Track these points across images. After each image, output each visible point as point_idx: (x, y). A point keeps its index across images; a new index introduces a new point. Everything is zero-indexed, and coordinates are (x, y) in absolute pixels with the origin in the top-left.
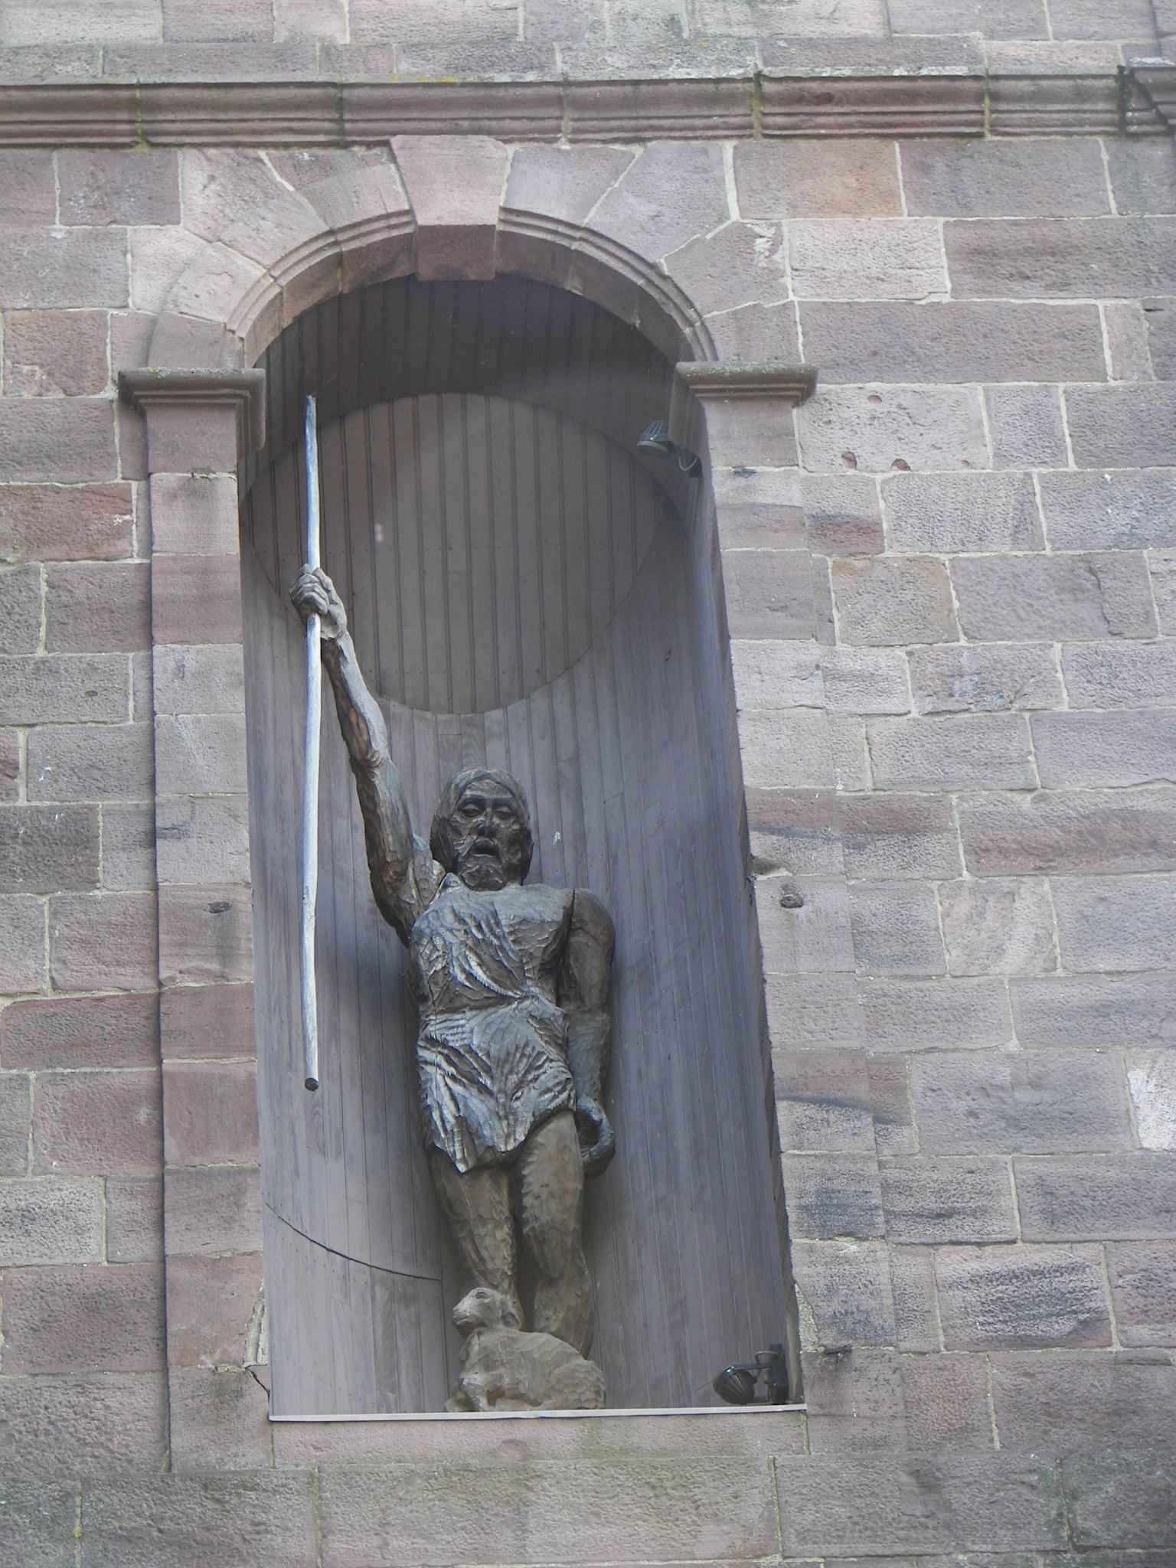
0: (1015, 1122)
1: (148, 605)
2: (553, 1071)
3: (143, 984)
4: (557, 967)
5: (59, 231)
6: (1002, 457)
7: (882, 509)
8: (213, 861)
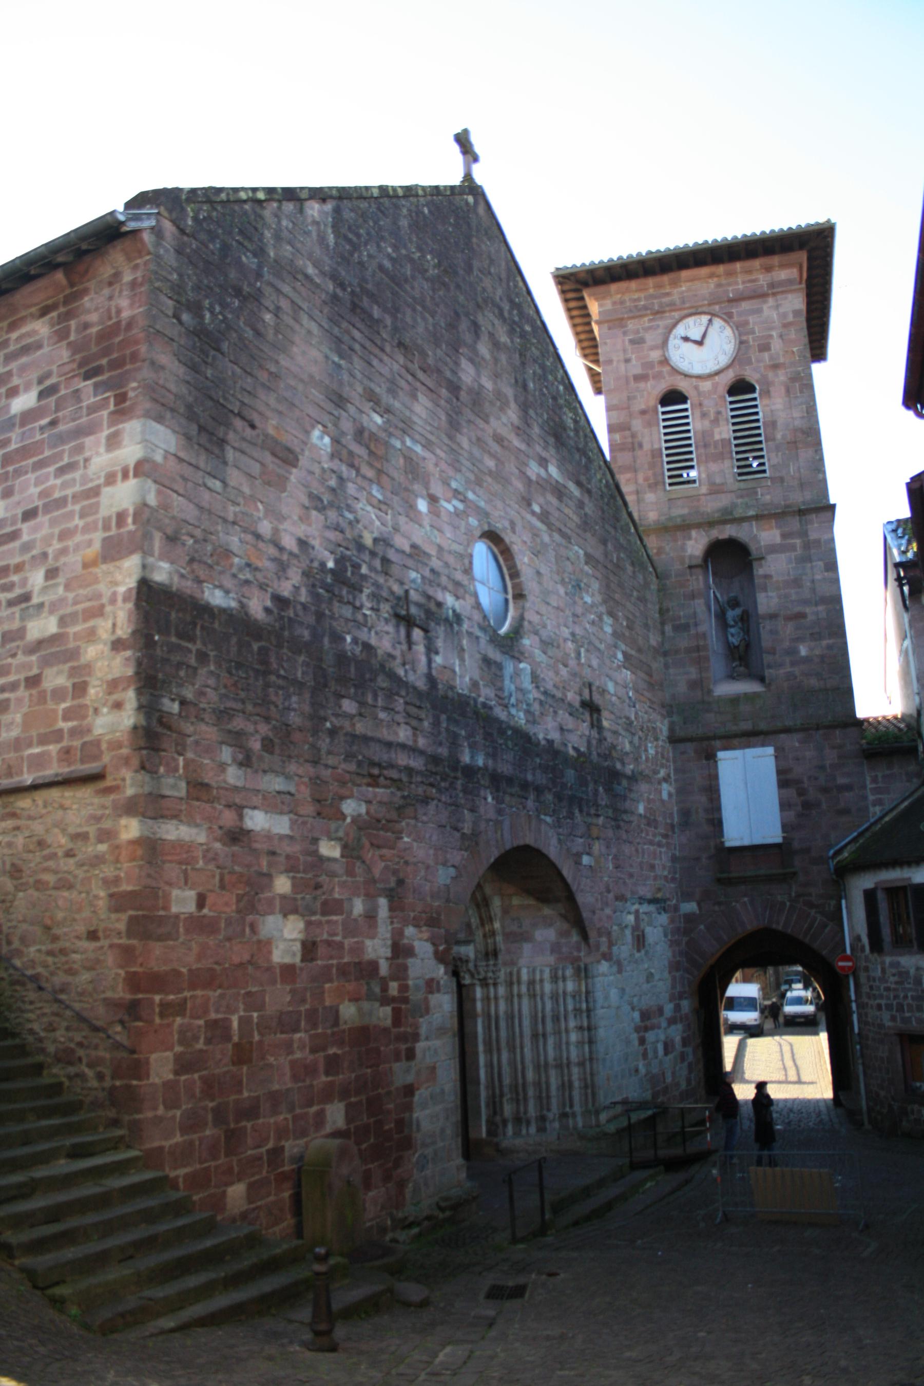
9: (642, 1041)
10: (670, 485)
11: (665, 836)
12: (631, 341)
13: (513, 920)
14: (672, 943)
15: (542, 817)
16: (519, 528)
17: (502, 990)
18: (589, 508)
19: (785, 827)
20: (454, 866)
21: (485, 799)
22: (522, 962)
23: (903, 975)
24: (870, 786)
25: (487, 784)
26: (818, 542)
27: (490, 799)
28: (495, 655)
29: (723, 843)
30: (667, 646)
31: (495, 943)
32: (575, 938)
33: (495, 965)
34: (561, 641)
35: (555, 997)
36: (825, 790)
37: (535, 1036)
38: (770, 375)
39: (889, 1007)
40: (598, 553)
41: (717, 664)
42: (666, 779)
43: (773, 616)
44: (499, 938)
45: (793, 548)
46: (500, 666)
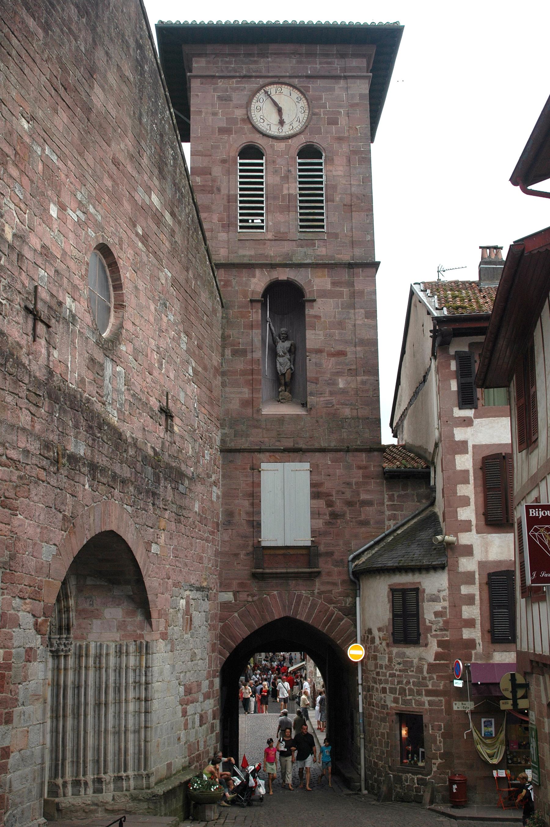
0: (328, 384)
1: (252, 325)
2: (289, 364)
3: (251, 368)
4: (290, 351)
5: (244, 279)
6: (334, 309)
7: (322, 315)
8: (258, 355)
9: (184, 713)
10: (241, 227)
11: (212, 533)
12: (219, 97)
13: (86, 598)
14: (212, 627)
15: (125, 506)
16: (125, 246)
17: (71, 662)
18: (178, 238)
19: (314, 533)
20: (55, 545)
21: (84, 486)
22: (92, 637)
23: (407, 665)
24: (387, 503)
25: (86, 472)
26: (362, 293)
27: (87, 486)
28: (99, 356)
29: (259, 542)
30: (225, 368)
31: (68, 618)
32: (139, 618)
33: (67, 639)
34: (149, 352)
35: (118, 670)
36: (350, 504)
37: (98, 705)
38: (336, 146)
39: (393, 691)
40: (181, 279)
41: (266, 388)
42: (215, 484)
43: (319, 351)
44: (72, 614)
45: (341, 295)
46: (102, 366)
